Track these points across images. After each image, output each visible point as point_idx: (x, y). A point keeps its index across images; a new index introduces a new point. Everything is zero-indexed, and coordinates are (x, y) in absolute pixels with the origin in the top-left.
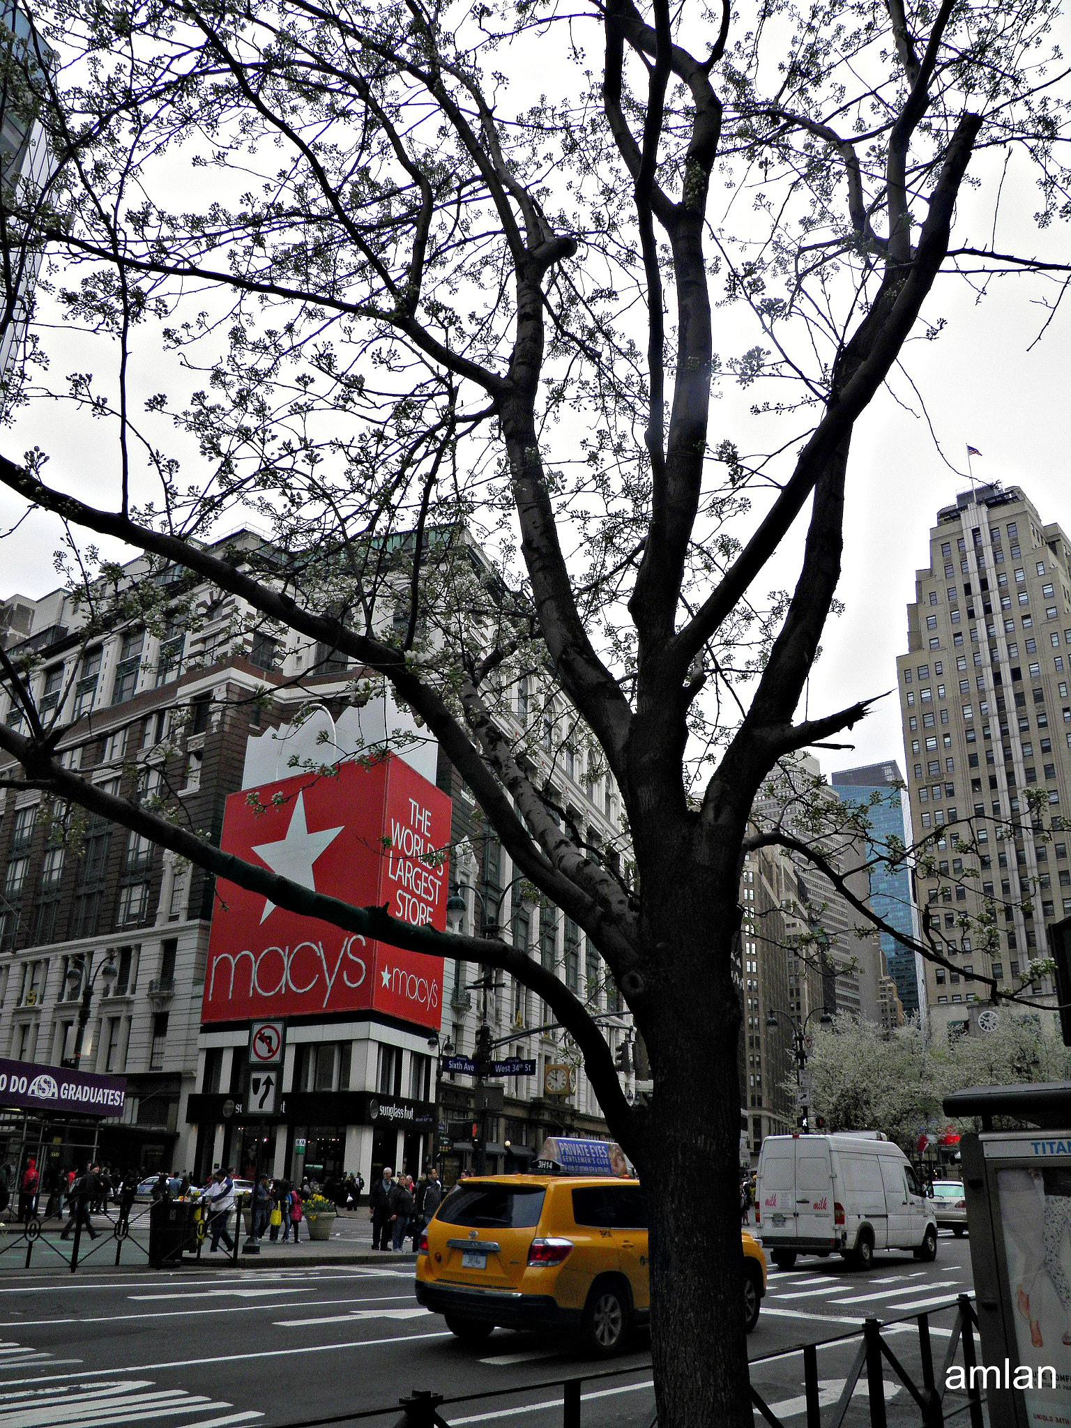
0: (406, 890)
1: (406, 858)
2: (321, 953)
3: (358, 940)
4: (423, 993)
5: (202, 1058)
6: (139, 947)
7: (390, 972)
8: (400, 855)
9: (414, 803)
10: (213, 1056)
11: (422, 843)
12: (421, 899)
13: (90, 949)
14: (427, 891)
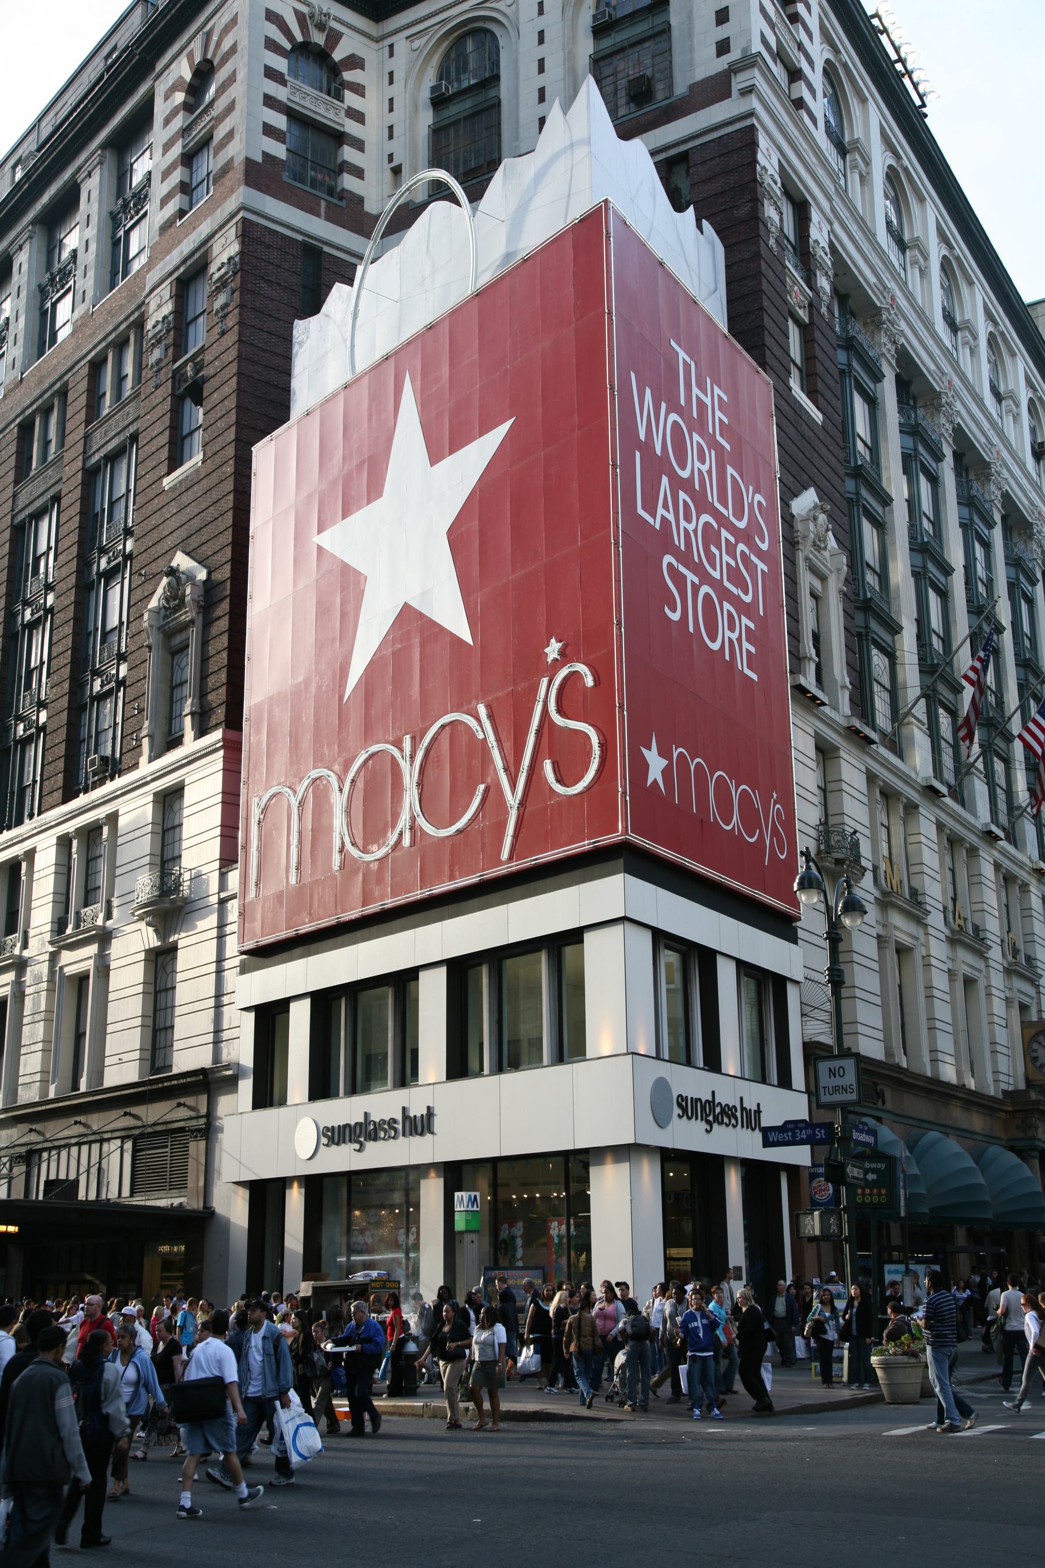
0: (685, 558)
1: (678, 484)
2: (483, 728)
3: (574, 675)
4: (751, 819)
6: (113, 818)
7: (664, 752)
8: (656, 466)
9: (682, 355)
10: (270, 1018)
11: (711, 456)
12: (725, 595)
13: (27, 845)
14: (734, 575)
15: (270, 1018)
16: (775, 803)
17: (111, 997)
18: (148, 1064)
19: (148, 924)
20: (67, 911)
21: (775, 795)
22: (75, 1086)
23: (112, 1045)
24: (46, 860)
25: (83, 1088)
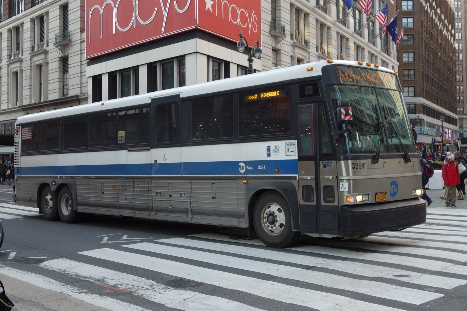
5: (90, 82)
10: (97, 80)
13: (21, 21)
15: (97, 80)
16: (254, 14)
17: (49, 72)
18: (62, 93)
19: (59, 49)
20: (35, 44)
21: (254, 12)
22: (40, 100)
23: (51, 87)
24: (27, 26)
25: (42, 101)
